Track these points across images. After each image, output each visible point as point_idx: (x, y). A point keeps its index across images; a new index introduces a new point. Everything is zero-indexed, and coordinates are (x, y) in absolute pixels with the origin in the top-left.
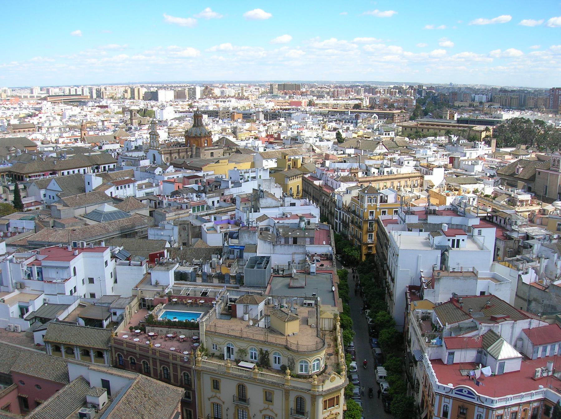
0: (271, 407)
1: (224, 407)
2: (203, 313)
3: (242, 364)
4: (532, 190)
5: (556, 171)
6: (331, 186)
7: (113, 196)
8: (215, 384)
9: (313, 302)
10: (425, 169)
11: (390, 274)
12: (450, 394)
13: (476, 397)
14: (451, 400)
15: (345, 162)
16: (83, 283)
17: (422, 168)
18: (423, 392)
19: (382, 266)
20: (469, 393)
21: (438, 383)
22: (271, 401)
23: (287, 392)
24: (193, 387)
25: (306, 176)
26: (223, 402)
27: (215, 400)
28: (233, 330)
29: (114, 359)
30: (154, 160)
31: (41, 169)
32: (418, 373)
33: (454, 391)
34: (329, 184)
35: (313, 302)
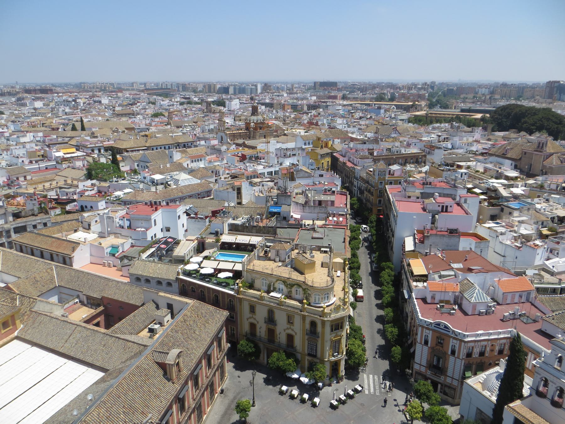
0: (292, 327)
1: (258, 327)
2: (247, 255)
3: (272, 294)
4: (518, 167)
5: (541, 152)
7: (190, 167)
9: (328, 250)
10: (428, 150)
11: (392, 230)
12: (430, 327)
13: (451, 331)
14: (431, 332)
15: (365, 143)
16: (162, 231)
17: (426, 149)
18: (410, 323)
19: (387, 224)
20: (446, 327)
21: (420, 317)
23: (304, 317)
25: (335, 154)
27: (252, 321)
28: (267, 269)
30: (222, 140)
31: (136, 146)
32: (408, 309)
33: (433, 325)
34: (351, 159)
35: (328, 250)
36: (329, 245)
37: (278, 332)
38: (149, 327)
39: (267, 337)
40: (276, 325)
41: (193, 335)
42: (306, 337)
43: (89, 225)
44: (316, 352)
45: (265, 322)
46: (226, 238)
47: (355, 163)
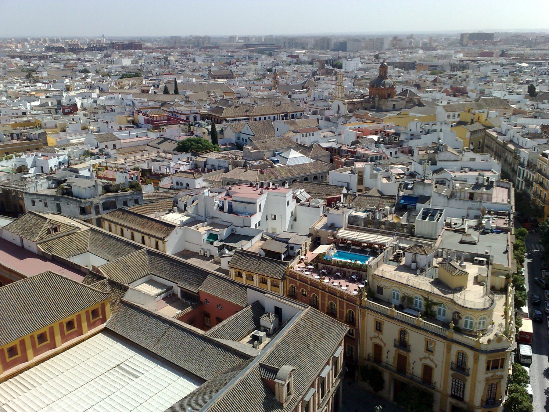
0: (431, 356)
6: (517, 142)
8: (378, 325)
15: (535, 117)
16: (267, 219)
22: (432, 352)
24: (357, 325)
26: (385, 344)
27: (377, 341)
29: (288, 289)
34: (515, 140)
36: (487, 253)
37: (411, 361)
38: (253, 333)
39: (395, 365)
40: (409, 351)
41: (307, 350)
42: (451, 372)
43: (185, 206)
44: (463, 395)
45: (395, 346)
46: (342, 233)
47: (520, 144)
